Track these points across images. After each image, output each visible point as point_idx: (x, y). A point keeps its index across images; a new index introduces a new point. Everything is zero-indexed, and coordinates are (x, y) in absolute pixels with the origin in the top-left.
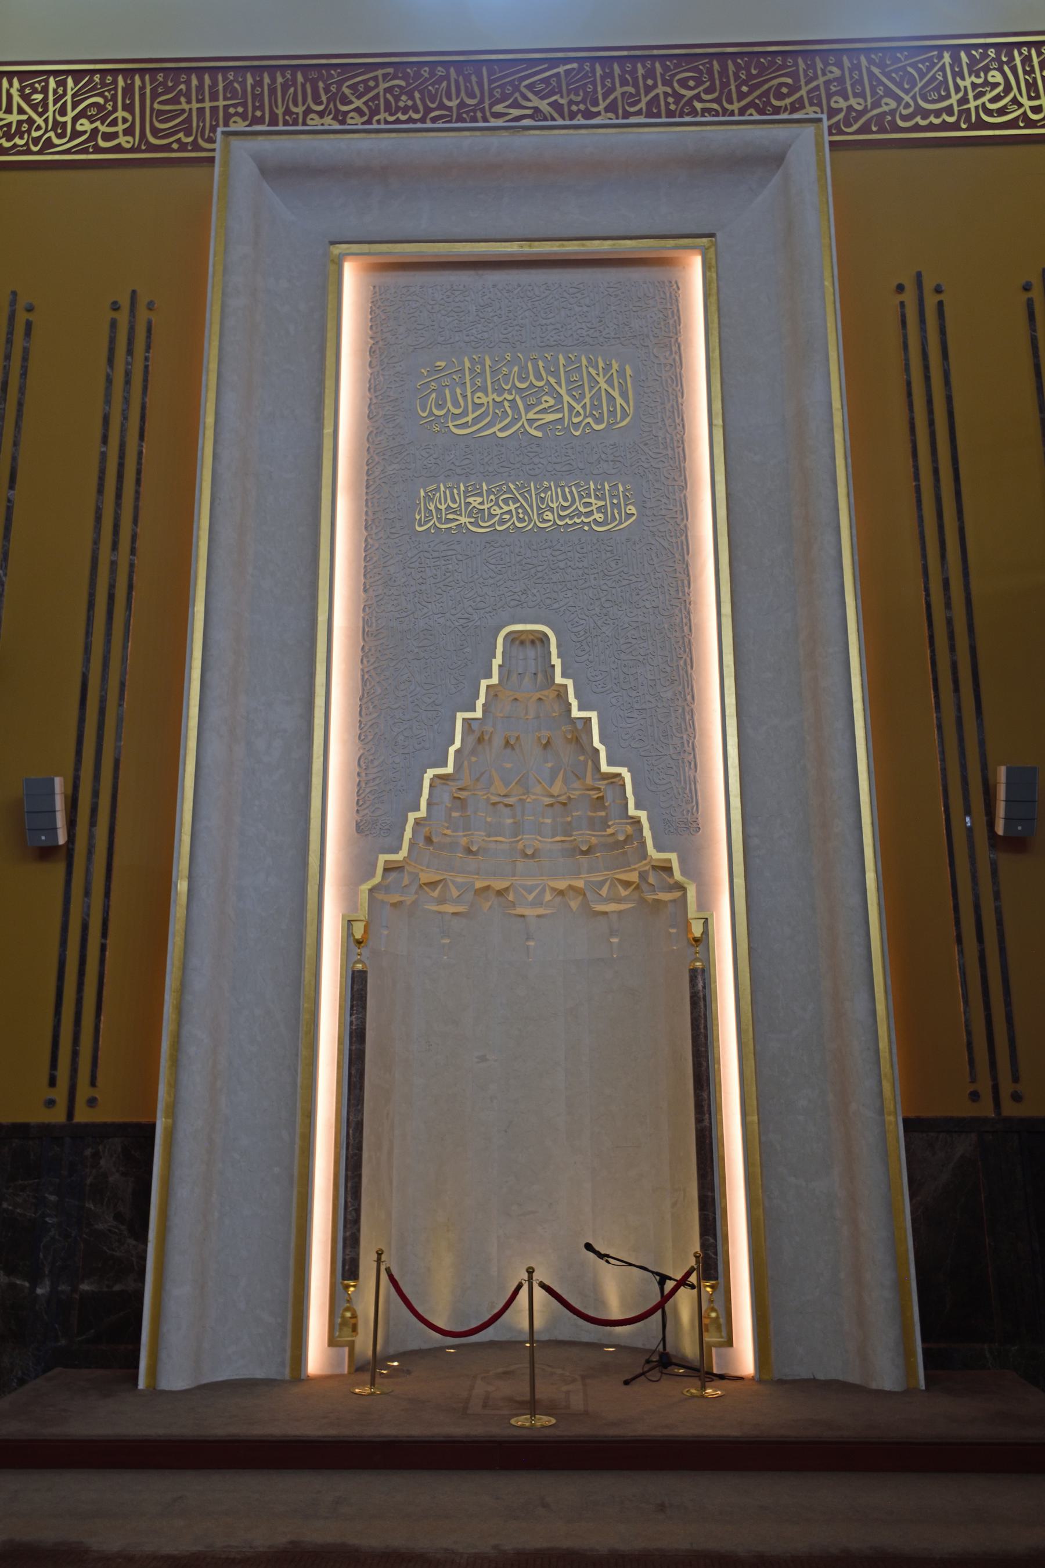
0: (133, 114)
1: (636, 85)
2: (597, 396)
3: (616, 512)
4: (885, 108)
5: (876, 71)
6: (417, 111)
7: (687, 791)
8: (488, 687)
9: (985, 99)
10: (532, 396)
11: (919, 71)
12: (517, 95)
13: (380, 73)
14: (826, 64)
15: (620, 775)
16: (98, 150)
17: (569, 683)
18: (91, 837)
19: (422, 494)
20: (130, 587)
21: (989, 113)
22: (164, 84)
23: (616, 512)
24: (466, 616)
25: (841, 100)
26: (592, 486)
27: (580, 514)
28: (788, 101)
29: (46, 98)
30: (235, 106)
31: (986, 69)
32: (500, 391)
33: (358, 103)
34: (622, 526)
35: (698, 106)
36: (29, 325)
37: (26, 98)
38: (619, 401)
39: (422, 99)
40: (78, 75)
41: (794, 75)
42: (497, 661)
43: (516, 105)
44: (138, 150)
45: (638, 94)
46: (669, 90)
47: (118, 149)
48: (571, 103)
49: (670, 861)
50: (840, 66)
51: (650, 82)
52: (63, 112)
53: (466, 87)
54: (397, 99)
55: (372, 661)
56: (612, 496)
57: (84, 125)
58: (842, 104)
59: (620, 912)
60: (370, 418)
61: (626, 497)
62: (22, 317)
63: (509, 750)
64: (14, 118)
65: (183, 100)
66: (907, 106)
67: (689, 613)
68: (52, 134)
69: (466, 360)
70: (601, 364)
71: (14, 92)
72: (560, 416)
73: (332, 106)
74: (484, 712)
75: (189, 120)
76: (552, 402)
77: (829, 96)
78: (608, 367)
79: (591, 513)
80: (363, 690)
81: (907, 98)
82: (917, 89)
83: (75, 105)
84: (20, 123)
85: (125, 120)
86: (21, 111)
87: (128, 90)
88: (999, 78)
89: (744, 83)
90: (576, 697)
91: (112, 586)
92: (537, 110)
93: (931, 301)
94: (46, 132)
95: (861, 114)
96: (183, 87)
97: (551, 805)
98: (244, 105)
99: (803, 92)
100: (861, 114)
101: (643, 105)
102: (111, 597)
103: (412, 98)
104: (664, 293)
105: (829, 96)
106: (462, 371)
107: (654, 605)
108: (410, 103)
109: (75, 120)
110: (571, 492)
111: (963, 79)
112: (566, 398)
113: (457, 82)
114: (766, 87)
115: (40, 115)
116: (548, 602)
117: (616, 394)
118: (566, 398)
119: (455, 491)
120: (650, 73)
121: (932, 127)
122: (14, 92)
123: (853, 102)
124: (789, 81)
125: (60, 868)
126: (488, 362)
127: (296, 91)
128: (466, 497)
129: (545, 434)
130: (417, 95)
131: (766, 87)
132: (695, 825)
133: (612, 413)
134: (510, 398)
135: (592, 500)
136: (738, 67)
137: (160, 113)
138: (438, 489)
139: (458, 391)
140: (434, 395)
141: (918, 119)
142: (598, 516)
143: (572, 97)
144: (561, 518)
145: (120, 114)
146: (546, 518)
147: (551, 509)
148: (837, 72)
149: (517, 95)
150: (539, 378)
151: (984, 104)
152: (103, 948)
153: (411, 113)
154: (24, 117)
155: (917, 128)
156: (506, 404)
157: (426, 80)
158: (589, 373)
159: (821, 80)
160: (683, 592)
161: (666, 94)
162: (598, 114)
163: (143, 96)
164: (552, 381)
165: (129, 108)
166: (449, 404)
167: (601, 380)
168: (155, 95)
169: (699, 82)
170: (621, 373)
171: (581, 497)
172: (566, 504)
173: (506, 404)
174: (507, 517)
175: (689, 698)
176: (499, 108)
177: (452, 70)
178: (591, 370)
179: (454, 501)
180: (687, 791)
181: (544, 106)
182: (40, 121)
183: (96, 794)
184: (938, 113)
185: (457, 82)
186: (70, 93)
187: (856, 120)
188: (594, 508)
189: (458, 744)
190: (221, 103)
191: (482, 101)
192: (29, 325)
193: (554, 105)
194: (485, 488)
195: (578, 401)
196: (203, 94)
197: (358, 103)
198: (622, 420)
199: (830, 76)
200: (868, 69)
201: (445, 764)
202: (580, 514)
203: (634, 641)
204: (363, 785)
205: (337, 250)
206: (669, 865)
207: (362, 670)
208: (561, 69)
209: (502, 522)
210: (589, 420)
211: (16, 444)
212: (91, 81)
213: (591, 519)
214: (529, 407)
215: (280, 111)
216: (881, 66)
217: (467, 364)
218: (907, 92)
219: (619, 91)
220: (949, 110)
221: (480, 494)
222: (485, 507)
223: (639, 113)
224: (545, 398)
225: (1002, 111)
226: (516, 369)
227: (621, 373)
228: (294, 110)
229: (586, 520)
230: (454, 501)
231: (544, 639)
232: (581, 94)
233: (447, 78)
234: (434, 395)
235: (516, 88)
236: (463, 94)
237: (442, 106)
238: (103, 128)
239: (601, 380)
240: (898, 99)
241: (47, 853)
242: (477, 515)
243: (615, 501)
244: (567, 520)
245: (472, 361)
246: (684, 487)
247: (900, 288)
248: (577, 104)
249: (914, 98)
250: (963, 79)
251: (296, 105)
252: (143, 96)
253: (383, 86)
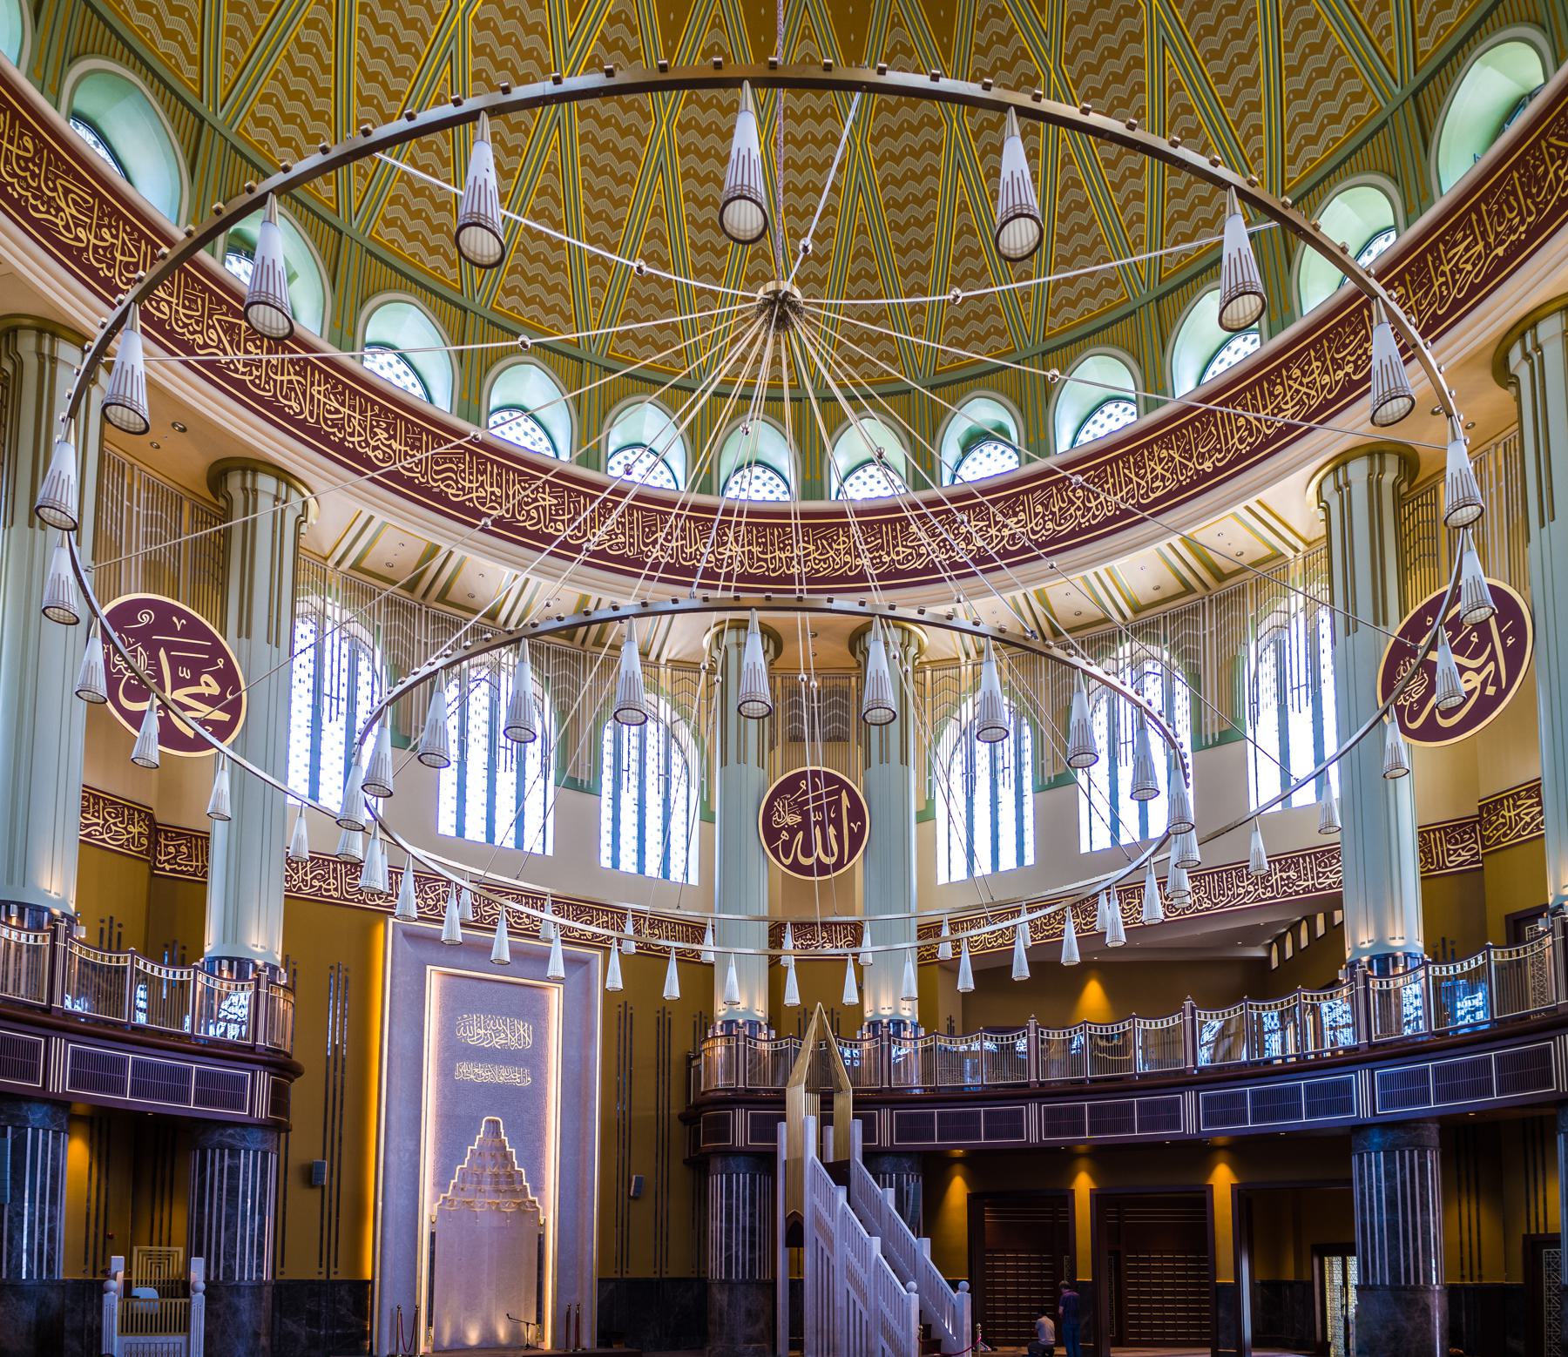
16: (322, 896)
47: (331, 897)
52: (306, 875)
57: (315, 882)
87: (335, 870)
91: (335, 1086)
102: (335, 1090)
145: (332, 880)
165: (335, 879)
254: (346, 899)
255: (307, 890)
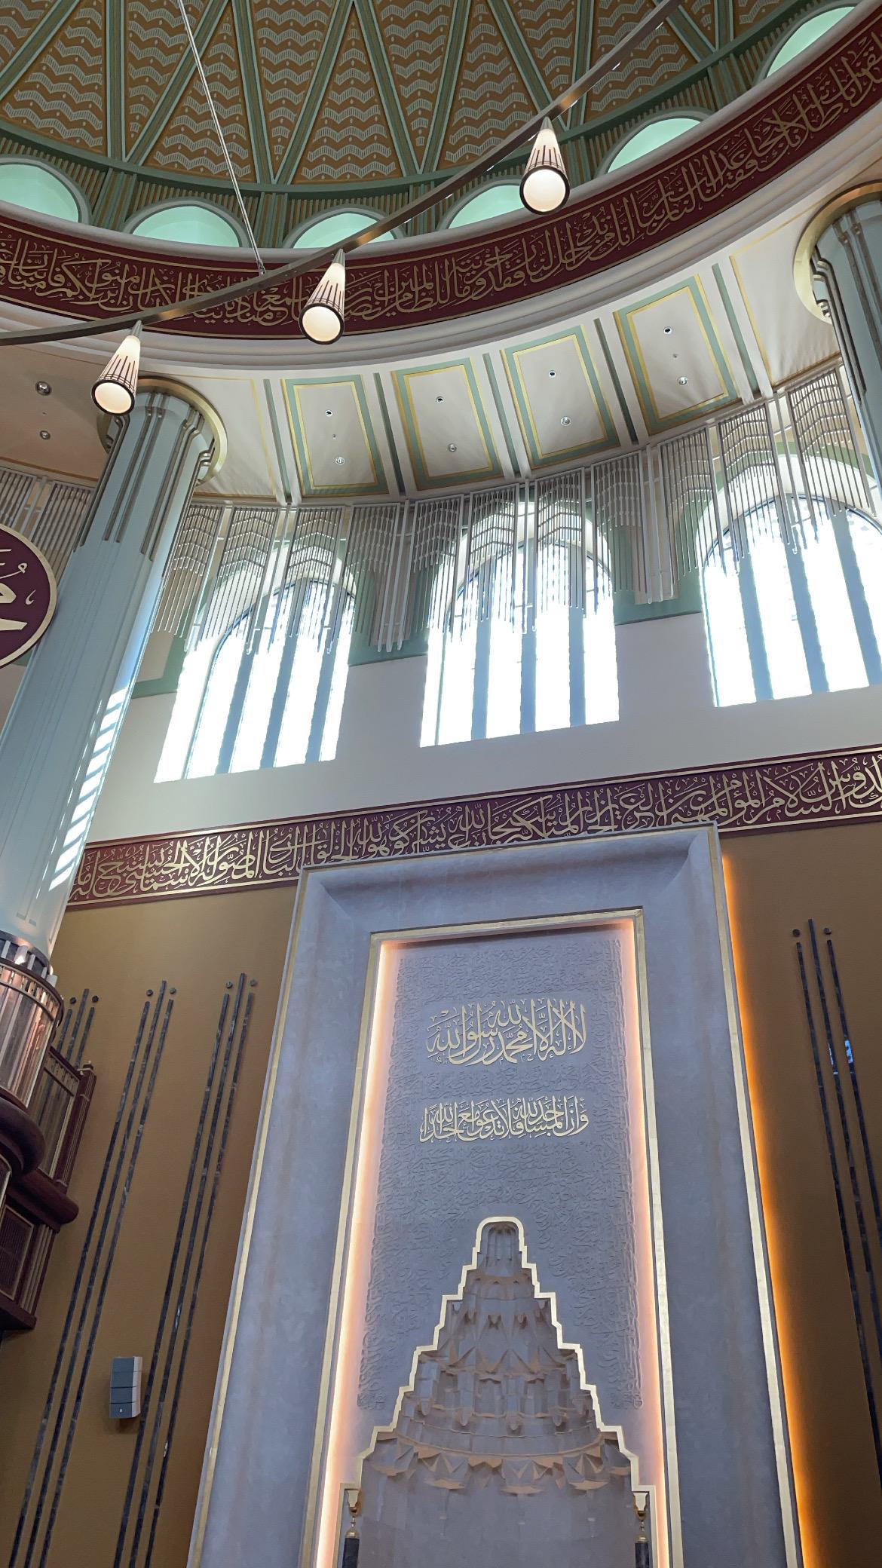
0: (256, 856)
1: (593, 804)
2: (559, 1029)
3: (572, 1120)
4: (777, 805)
5: (768, 780)
6: (441, 836)
7: (631, 1366)
8: (469, 1272)
9: (853, 792)
10: (510, 1032)
11: (800, 777)
12: (510, 819)
13: (418, 814)
14: (730, 779)
15: (574, 1351)
16: (231, 881)
17: (533, 1267)
18: (159, 1410)
19: (426, 1112)
20: (213, 1196)
21: (857, 801)
22: (278, 835)
23: (572, 1120)
24: (455, 1211)
25: (742, 802)
26: (554, 1100)
27: (544, 1123)
28: (703, 806)
29: (203, 851)
30: (322, 844)
31: (852, 772)
32: (486, 1029)
33: (403, 834)
34: (577, 1132)
35: (638, 815)
36: (171, 1003)
37: (190, 852)
38: (575, 1032)
39: (445, 828)
40: (223, 834)
41: (708, 789)
42: (476, 1249)
43: (510, 826)
44: (257, 879)
45: (594, 810)
46: (617, 807)
47: (245, 879)
48: (547, 821)
49: (615, 1434)
50: (740, 779)
51: (603, 802)
52: (212, 859)
53: (475, 817)
54: (429, 829)
55: (380, 1251)
56: (569, 1108)
57: (225, 866)
58: (744, 805)
59: (596, 1490)
60: (391, 1056)
61: (579, 1107)
62: (168, 997)
63: (493, 1329)
64: (182, 865)
65: (289, 843)
66: (793, 802)
67: (630, 1203)
68: (203, 874)
69: (463, 1008)
70: (562, 1005)
71: (184, 850)
72: (531, 1046)
73: (385, 838)
74: (465, 1293)
75: (292, 856)
76: (525, 1036)
77: (734, 800)
78: (568, 1006)
79: (553, 1122)
80: (372, 1276)
81: (792, 797)
82: (799, 790)
83: (220, 854)
84: (184, 869)
85: (250, 860)
86: (186, 861)
88: (862, 777)
89: (670, 797)
90: (538, 1280)
91: (201, 1196)
92: (524, 827)
93: (822, 942)
94: (200, 872)
95: (757, 810)
96: (290, 835)
97: (533, 1382)
98: (328, 843)
99: (714, 799)
100: (757, 810)
101: (598, 818)
102: (199, 1204)
103: (440, 829)
104: (609, 949)
105: (734, 800)
106: (460, 1016)
107: (603, 1197)
108: (437, 831)
109: (219, 863)
110: (538, 1106)
111: (834, 780)
112: (535, 1032)
113: (470, 815)
114: (686, 798)
115: (197, 862)
116: (519, 1197)
117: (573, 1027)
118: (535, 1032)
119: (451, 1109)
120: (603, 796)
121: (812, 815)
122: (184, 850)
123: (751, 802)
124: (704, 792)
125: (135, 1437)
126: (479, 1009)
127: (362, 831)
128: (458, 1113)
129: (519, 1060)
130: (442, 826)
131: (686, 798)
132: (638, 1399)
133: (570, 1042)
134: (494, 1034)
135: (554, 1111)
136: (666, 787)
137: (274, 853)
138: (437, 1108)
139: (457, 1031)
140: (439, 1036)
141: (802, 810)
142: (559, 1125)
143: (548, 817)
144: (530, 1127)
145: (248, 856)
146: (518, 1127)
147: (522, 1120)
148: (739, 784)
149: (510, 819)
150: (516, 1018)
151: (852, 795)
152: (156, 1513)
153: (438, 838)
154: (188, 865)
155: (801, 817)
156: (491, 1039)
157: (449, 815)
158: (553, 1012)
159: (727, 790)
160: (626, 1185)
161: (614, 809)
162: (567, 826)
163: (264, 843)
164: (526, 1019)
165: (254, 853)
166: (449, 1042)
167: (562, 1017)
168: (271, 842)
169: (638, 800)
170: (577, 1011)
171: (545, 1109)
172: (535, 1115)
173: (491, 1039)
174: (489, 1127)
175: (631, 1279)
176: (497, 829)
177: (467, 807)
178: (554, 1009)
179: (449, 1116)
180: (631, 1366)
181: (528, 824)
182: (197, 866)
183: (167, 1373)
184: (816, 805)
185: (470, 815)
186: (218, 846)
187: (754, 815)
188: (555, 1117)
189: (442, 1324)
190: (313, 843)
191: (486, 825)
192: (171, 1003)
193: (537, 824)
194: (473, 1105)
195: (544, 1034)
196: (302, 839)
197: (403, 834)
198: (577, 1047)
199: (734, 787)
200: (762, 780)
201: (431, 1343)
202: (544, 1123)
203: (585, 1229)
204: (365, 1361)
205: (375, 938)
206: (614, 1439)
207: (372, 1259)
208: (541, 800)
209: (485, 1132)
210: (552, 1048)
211: (150, 1090)
212: (233, 837)
213: (553, 1127)
214: (507, 1042)
215: (351, 845)
216: (771, 776)
217: (464, 1011)
218: (792, 792)
219: (581, 810)
220: (825, 802)
221: (469, 1111)
222: (473, 1120)
223: (595, 823)
224: (520, 1033)
225: (866, 800)
226: (499, 1012)
227: (577, 1011)
228: (360, 843)
229: (549, 1128)
230: (449, 1116)
231: (511, 1229)
232: (554, 814)
233: (463, 812)
234: (439, 1036)
235: (510, 815)
236: (473, 822)
237: (459, 831)
238: (236, 867)
239: (562, 1017)
240: (786, 798)
241: (125, 1424)
242: (467, 1126)
243: (572, 1112)
244: (534, 1129)
245: (467, 1008)
246: (625, 1099)
247: (796, 933)
248: (551, 821)
249: (797, 796)
250: (834, 780)
251: (362, 839)
252: (264, 843)
253: (420, 822)
254: (266, 877)
255: (208, 879)
